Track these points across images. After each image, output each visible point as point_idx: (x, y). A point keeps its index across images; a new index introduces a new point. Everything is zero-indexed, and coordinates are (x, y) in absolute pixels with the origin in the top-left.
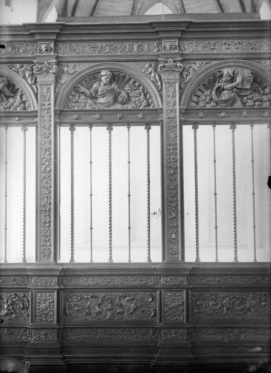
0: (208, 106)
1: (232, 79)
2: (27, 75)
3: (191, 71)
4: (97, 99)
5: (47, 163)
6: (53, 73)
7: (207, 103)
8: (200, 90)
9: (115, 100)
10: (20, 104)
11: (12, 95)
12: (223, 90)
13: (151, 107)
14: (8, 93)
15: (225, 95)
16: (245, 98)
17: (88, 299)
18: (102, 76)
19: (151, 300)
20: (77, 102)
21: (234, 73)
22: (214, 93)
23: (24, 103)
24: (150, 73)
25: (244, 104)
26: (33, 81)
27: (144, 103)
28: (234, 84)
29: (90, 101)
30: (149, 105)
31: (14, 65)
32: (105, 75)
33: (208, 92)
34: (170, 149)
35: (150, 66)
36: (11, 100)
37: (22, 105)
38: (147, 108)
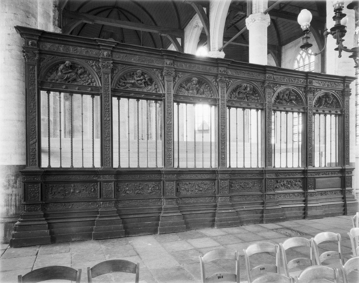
0: (235, 99)
1: (246, 88)
3: (230, 83)
4: (189, 91)
6: (173, 76)
10: (155, 89)
12: (241, 93)
13: (213, 98)
14: (149, 83)
15: (241, 96)
16: (248, 98)
18: (194, 80)
20: (181, 91)
21: (247, 86)
22: (237, 94)
24: (214, 82)
25: (248, 100)
27: (210, 95)
29: (187, 92)
30: (212, 96)
31: (153, 69)
32: (195, 79)
33: (234, 94)
35: (214, 78)
36: (150, 87)
38: (211, 98)
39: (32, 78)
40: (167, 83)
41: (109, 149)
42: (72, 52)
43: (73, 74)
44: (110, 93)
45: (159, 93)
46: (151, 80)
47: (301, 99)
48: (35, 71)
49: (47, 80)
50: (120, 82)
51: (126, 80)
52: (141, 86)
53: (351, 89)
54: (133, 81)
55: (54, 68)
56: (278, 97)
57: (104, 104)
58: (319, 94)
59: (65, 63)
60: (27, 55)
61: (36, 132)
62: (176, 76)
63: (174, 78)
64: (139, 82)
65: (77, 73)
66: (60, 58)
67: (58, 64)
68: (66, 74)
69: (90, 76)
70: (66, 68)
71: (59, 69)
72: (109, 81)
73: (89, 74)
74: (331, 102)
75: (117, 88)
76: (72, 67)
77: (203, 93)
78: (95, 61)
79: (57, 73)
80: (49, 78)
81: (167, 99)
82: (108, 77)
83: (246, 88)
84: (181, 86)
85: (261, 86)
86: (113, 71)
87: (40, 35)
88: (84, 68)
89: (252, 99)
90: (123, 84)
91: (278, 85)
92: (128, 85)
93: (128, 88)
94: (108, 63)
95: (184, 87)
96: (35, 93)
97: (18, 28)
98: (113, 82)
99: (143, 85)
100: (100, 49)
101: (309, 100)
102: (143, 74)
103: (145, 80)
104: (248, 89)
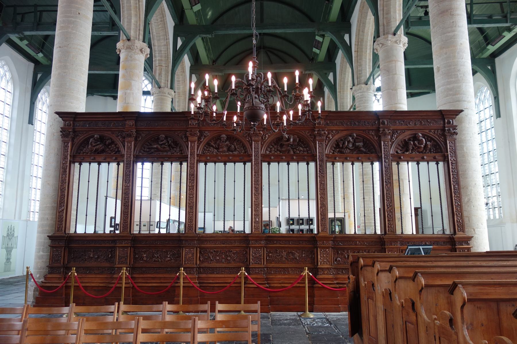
0: (276, 153)
2: (183, 137)
5: (192, 182)
7: (275, 152)
8: (272, 145)
9: (229, 150)
11: (175, 147)
12: (284, 145)
17: (212, 252)
19: (245, 253)
21: (288, 137)
23: (181, 151)
24: (246, 137)
25: (294, 152)
26: (186, 140)
27: (243, 151)
28: (289, 142)
34: (256, 175)
37: (180, 152)
38: (245, 154)
39: (66, 153)
40: (191, 144)
41: (128, 214)
42: (101, 127)
43: (101, 146)
44: (132, 159)
45: (184, 154)
46: (176, 144)
47: (373, 145)
48: (68, 147)
49: (80, 153)
50: (144, 148)
51: (151, 145)
52: (165, 149)
53: (456, 126)
54: (155, 146)
55: (86, 142)
56: (337, 146)
57: (126, 171)
58: (407, 135)
59: (94, 137)
60: (63, 134)
61: (64, 201)
62: (202, 136)
63: (199, 138)
64: (163, 146)
65: (105, 144)
66: (90, 132)
67: (89, 138)
68: (94, 146)
69: (117, 146)
70: (96, 140)
71: (90, 143)
72: (131, 149)
73: (116, 144)
74: (423, 146)
75: (141, 154)
76: (102, 139)
77: (235, 150)
78: (120, 132)
79: (88, 146)
80: (82, 152)
81: (190, 160)
82: (131, 145)
83: (288, 140)
84: (208, 144)
85: (310, 135)
86: (137, 138)
87: (74, 116)
88: (111, 139)
89: (300, 151)
90: (148, 150)
91: (334, 132)
92: (153, 150)
93: (152, 153)
94: (131, 132)
95: (212, 146)
96: (67, 166)
97: (57, 113)
98: (136, 149)
99: (168, 148)
100: (126, 120)
101: (384, 145)
102: (166, 138)
103: (168, 143)
104: (292, 140)
